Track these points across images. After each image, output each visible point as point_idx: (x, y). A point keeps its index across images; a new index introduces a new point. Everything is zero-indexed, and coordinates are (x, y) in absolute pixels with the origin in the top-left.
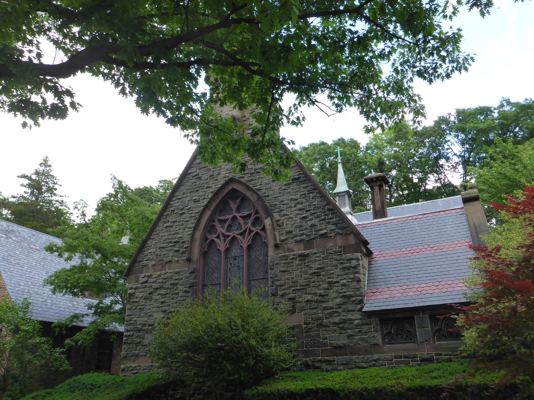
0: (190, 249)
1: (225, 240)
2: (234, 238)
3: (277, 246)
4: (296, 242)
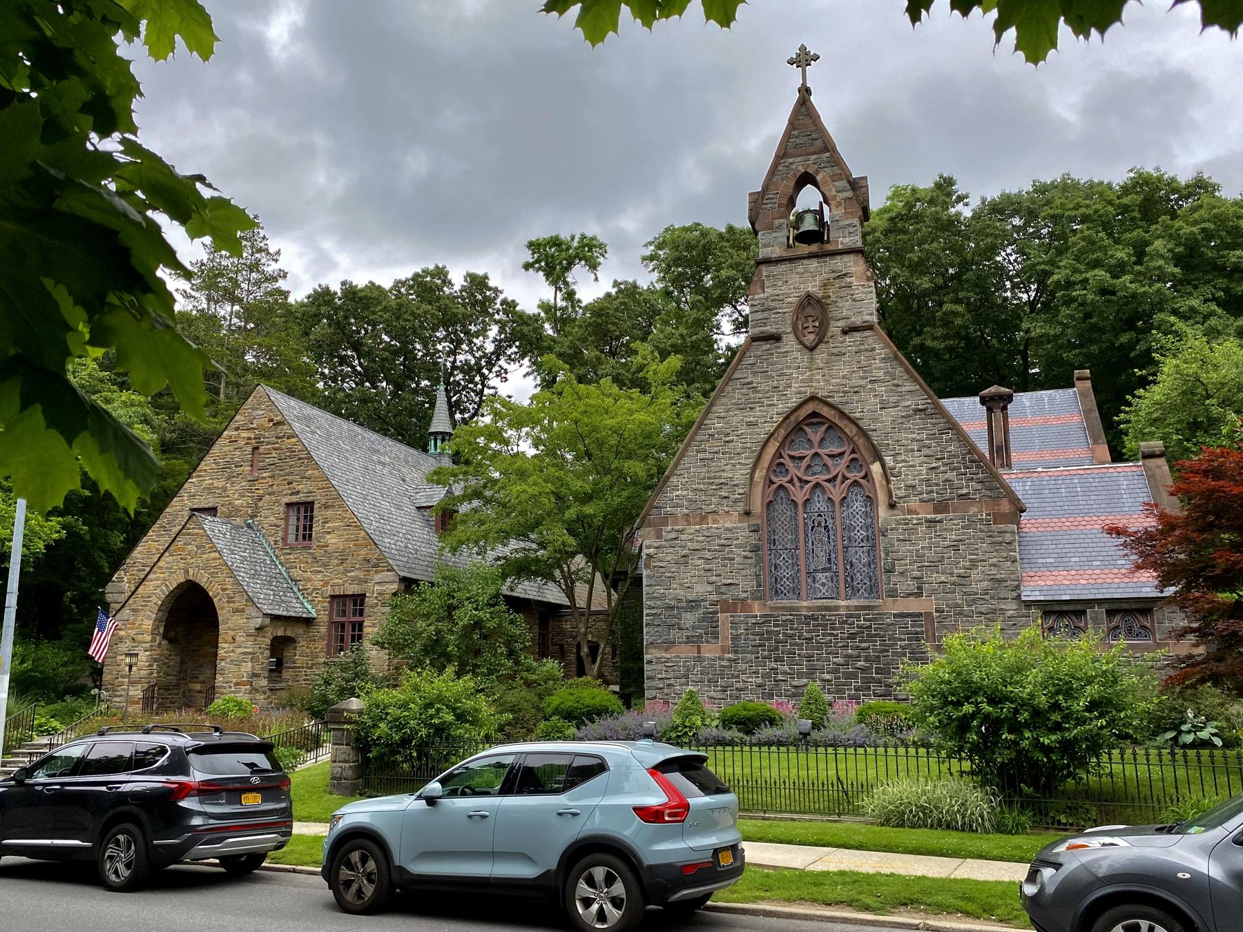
0: (748, 496)
1: (802, 488)
2: (817, 485)
3: (892, 506)
4: (922, 501)
